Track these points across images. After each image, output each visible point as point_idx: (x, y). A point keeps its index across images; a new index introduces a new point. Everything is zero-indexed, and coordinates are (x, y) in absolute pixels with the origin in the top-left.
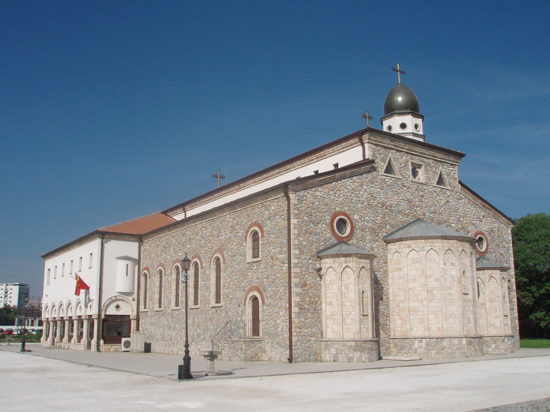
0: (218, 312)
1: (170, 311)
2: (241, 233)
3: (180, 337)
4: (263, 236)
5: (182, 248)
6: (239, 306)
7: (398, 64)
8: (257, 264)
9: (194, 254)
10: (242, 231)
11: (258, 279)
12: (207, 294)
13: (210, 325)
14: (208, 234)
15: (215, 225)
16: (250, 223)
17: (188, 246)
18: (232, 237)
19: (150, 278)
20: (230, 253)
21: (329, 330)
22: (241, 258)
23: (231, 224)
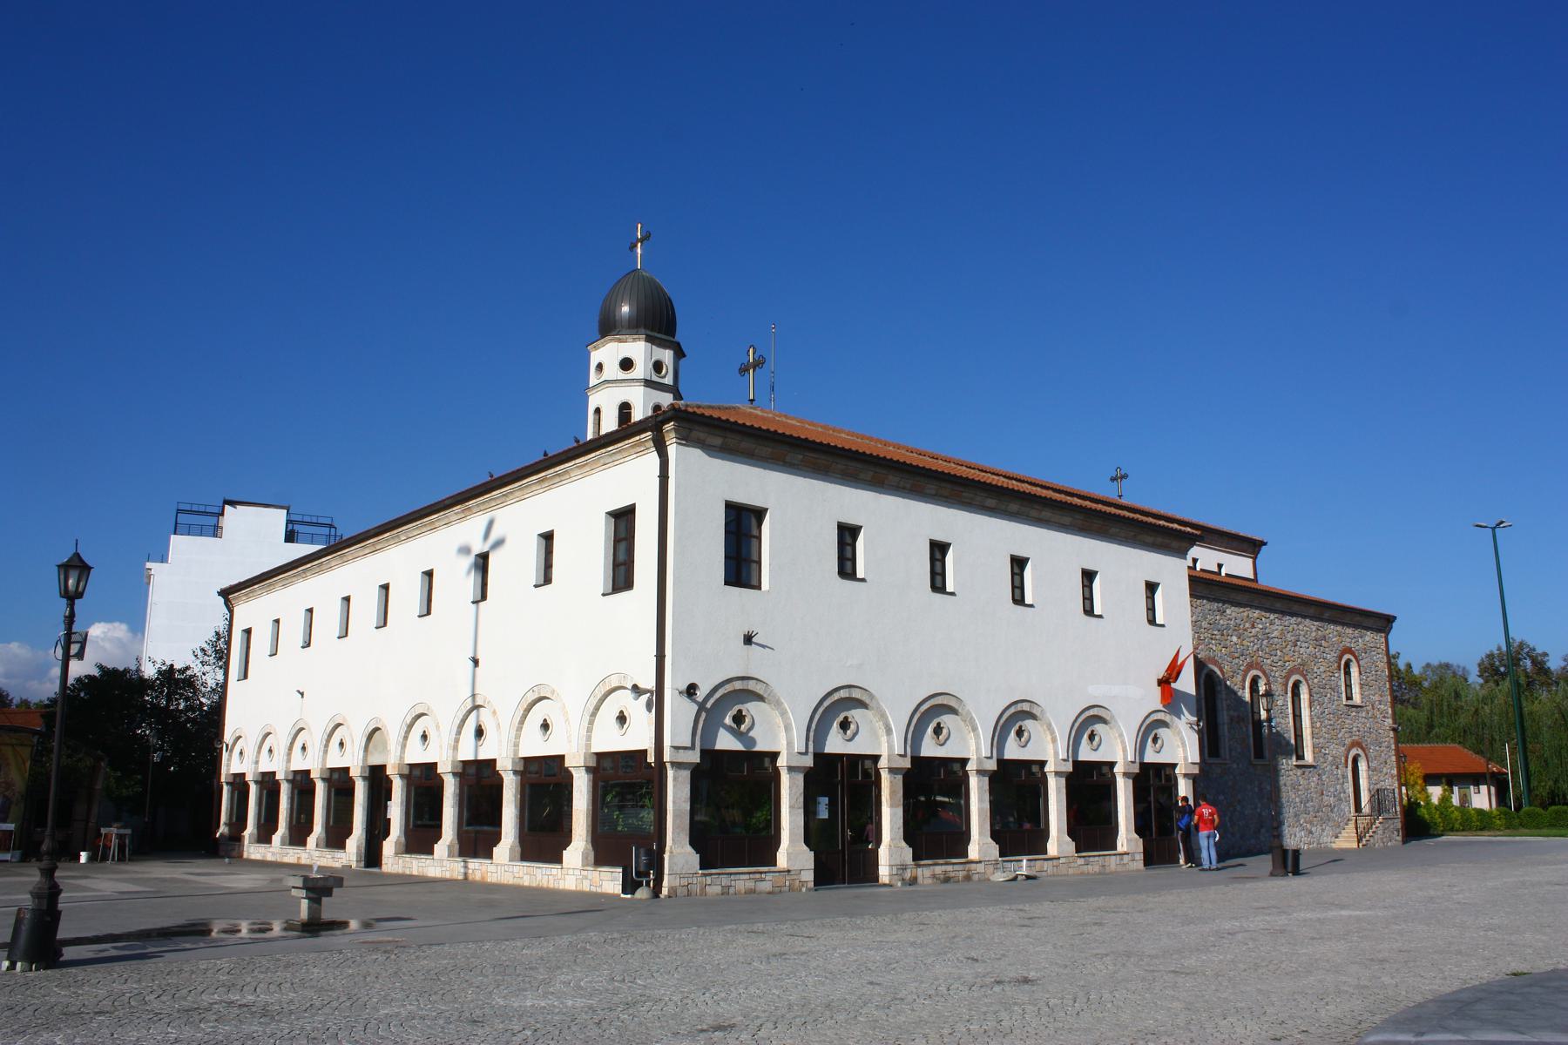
0: (1307, 773)
7: (639, 225)
11: (1359, 731)
13: (1294, 796)
17: (1234, 639)
23: (1314, 634)
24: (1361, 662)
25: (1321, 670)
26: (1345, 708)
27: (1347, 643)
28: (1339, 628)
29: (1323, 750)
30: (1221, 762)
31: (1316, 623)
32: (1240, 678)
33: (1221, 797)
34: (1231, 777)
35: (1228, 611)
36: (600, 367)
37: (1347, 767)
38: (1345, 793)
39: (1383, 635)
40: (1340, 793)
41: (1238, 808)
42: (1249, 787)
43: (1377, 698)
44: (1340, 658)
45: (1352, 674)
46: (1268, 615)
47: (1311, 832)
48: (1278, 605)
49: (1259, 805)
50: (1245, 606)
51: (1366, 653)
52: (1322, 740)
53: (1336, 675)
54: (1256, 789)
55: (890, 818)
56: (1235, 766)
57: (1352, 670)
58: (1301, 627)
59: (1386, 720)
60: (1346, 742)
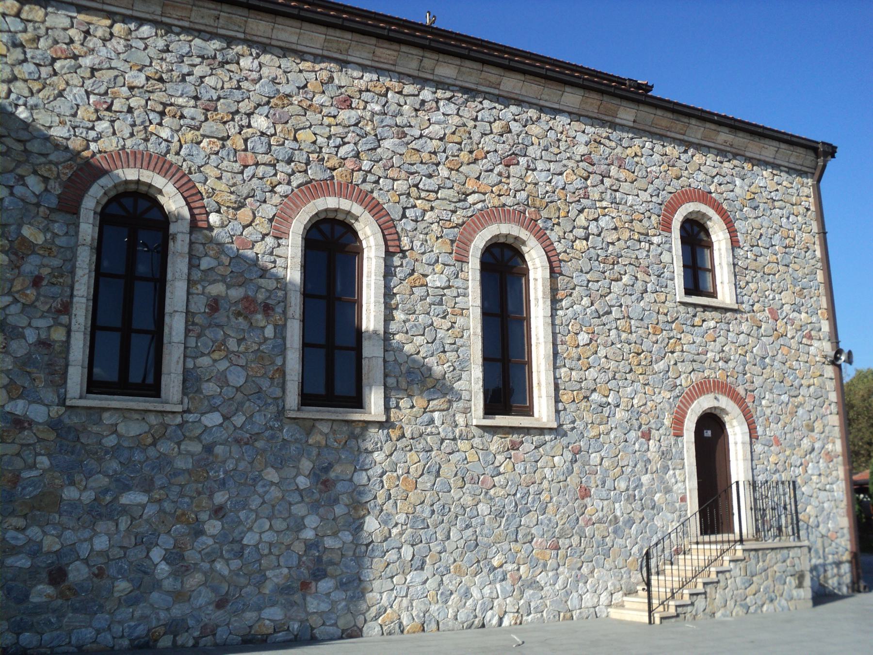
1: (38, 413)
3: (175, 557)
6: (647, 436)
10: (645, 196)
17: (260, 122)
18: (595, 194)
23: (582, 149)
24: (737, 225)
25: (603, 222)
26: (682, 309)
27: (697, 181)
28: (673, 151)
29: (595, 396)
30: (160, 407)
31: (589, 129)
32: (268, 210)
33: (133, 498)
34: (196, 448)
35: (245, 62)
37: (679, 435)
38: (668, 490)
39: (810, 181)
40: (652, 492)
41: (214, 527)
42: (271, 475)
43: (786, 297)
44: (672, 209)
45: (716, 246)
46: (409, 89)
47: (533, 584)
48: (447, 70)
49: (312, 521)
50: (318, 58)
51: (755, 208)
52: (592, 373)
53: (655, 240)
54: (303, 482)
56: (213, 419)
57: (714, 238)
58: (534, 129)
59: (816, 343)
60: (683, 381)
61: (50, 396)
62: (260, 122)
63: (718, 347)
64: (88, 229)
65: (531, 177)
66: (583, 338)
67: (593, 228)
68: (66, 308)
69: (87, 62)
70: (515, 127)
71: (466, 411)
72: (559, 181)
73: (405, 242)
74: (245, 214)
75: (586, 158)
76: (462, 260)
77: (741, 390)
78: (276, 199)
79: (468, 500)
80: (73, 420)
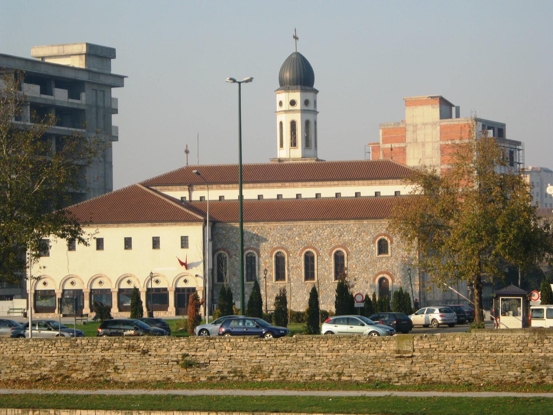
2: (368, 238)
4: (392, 242)
5: (287, 239)
6: (367, 282)
8: (386, 258)
9: (306, 245)
10: (369, 237)
11: (388, 267)
12: (326, 274)
14: (326, 234)
15: (335, 229)
16: (378, 233)
17: (297, 238)
18: (358, 239)
19: (231, 257)
20: (354, 249)
21: (428, 296)
22: (368, 253)
23: (355, 231)
32: (299, 252)
36: (281, 104)
42: (301, 291)
54: (305, 292)
55: (87, 303)
61: (271, 282)
62: (297, 238)
63: (386, 265)
64: (274, 259)
65: (344, 238)
66: (354, 266)
67: (357, 246)
68: (272, 270)
69: (271, 234)
70: (341, 229)
71: (332, 280)
72: (350, 238)
73: (321, 254)
74: (295, 253)
75: (357, 232)
76: (330, 255)
77: (391, 273)
78: (300, 250)
79: (331, 294)
80: (274, 285)
